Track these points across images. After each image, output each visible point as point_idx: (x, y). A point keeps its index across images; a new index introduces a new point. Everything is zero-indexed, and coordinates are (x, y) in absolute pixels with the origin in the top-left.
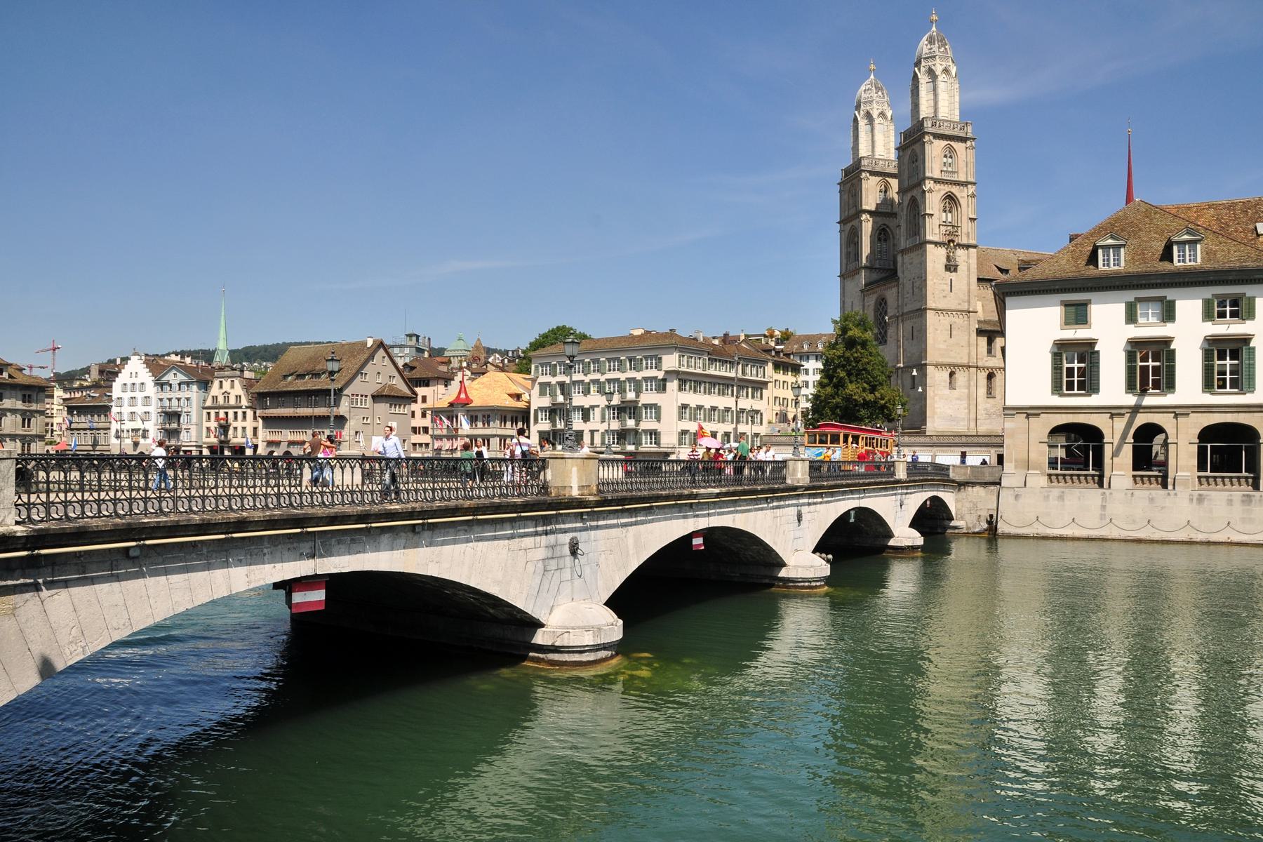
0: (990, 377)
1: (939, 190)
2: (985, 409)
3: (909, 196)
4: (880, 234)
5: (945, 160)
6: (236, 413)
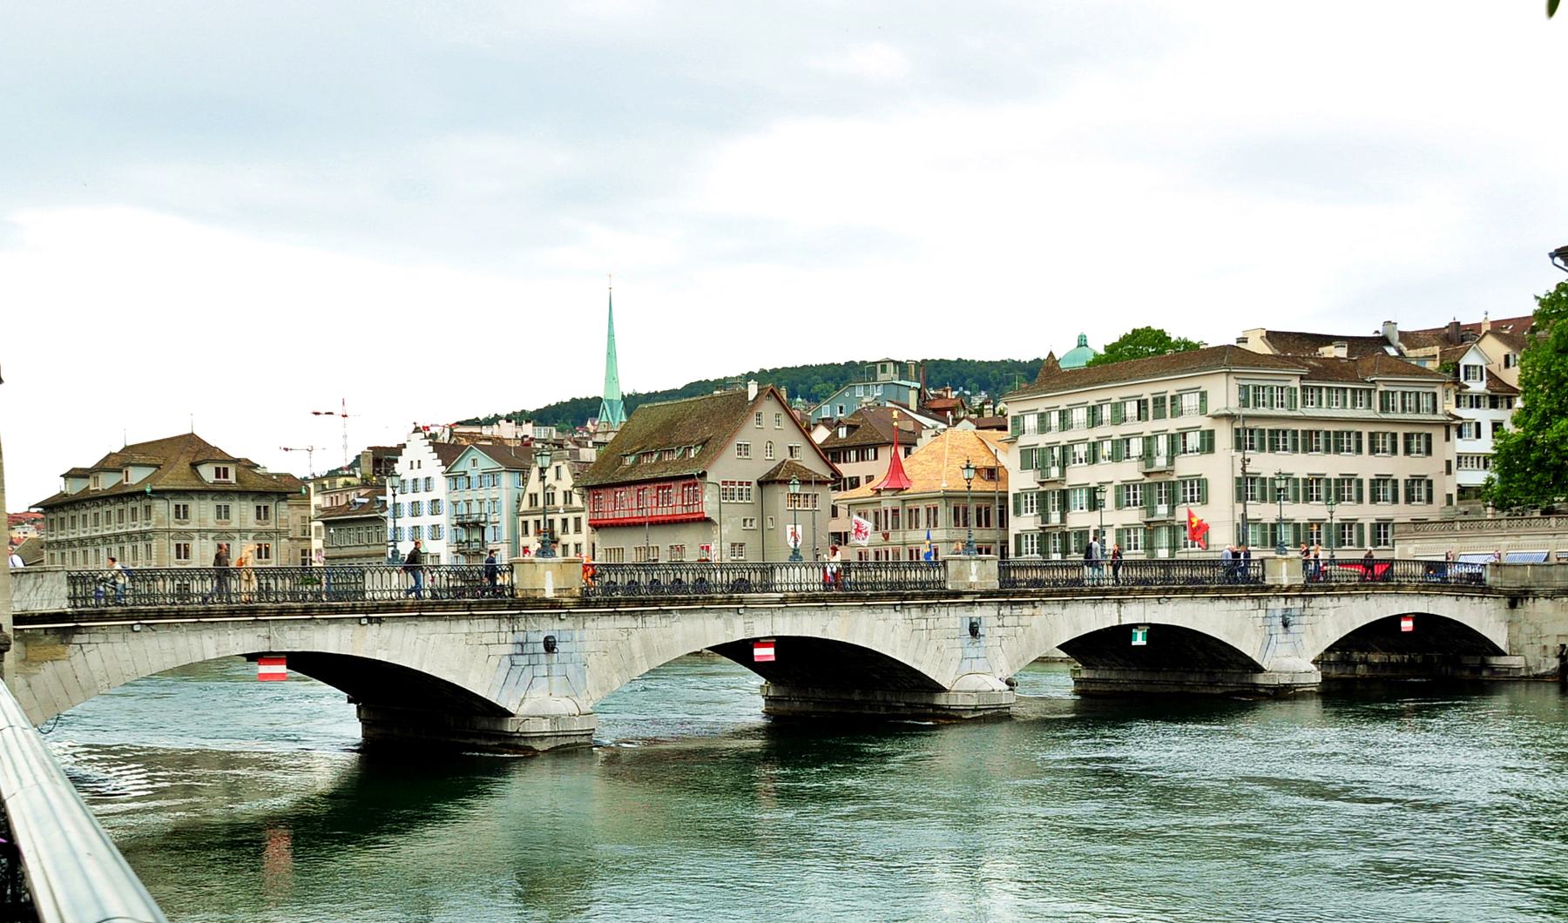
6: (565, 521)
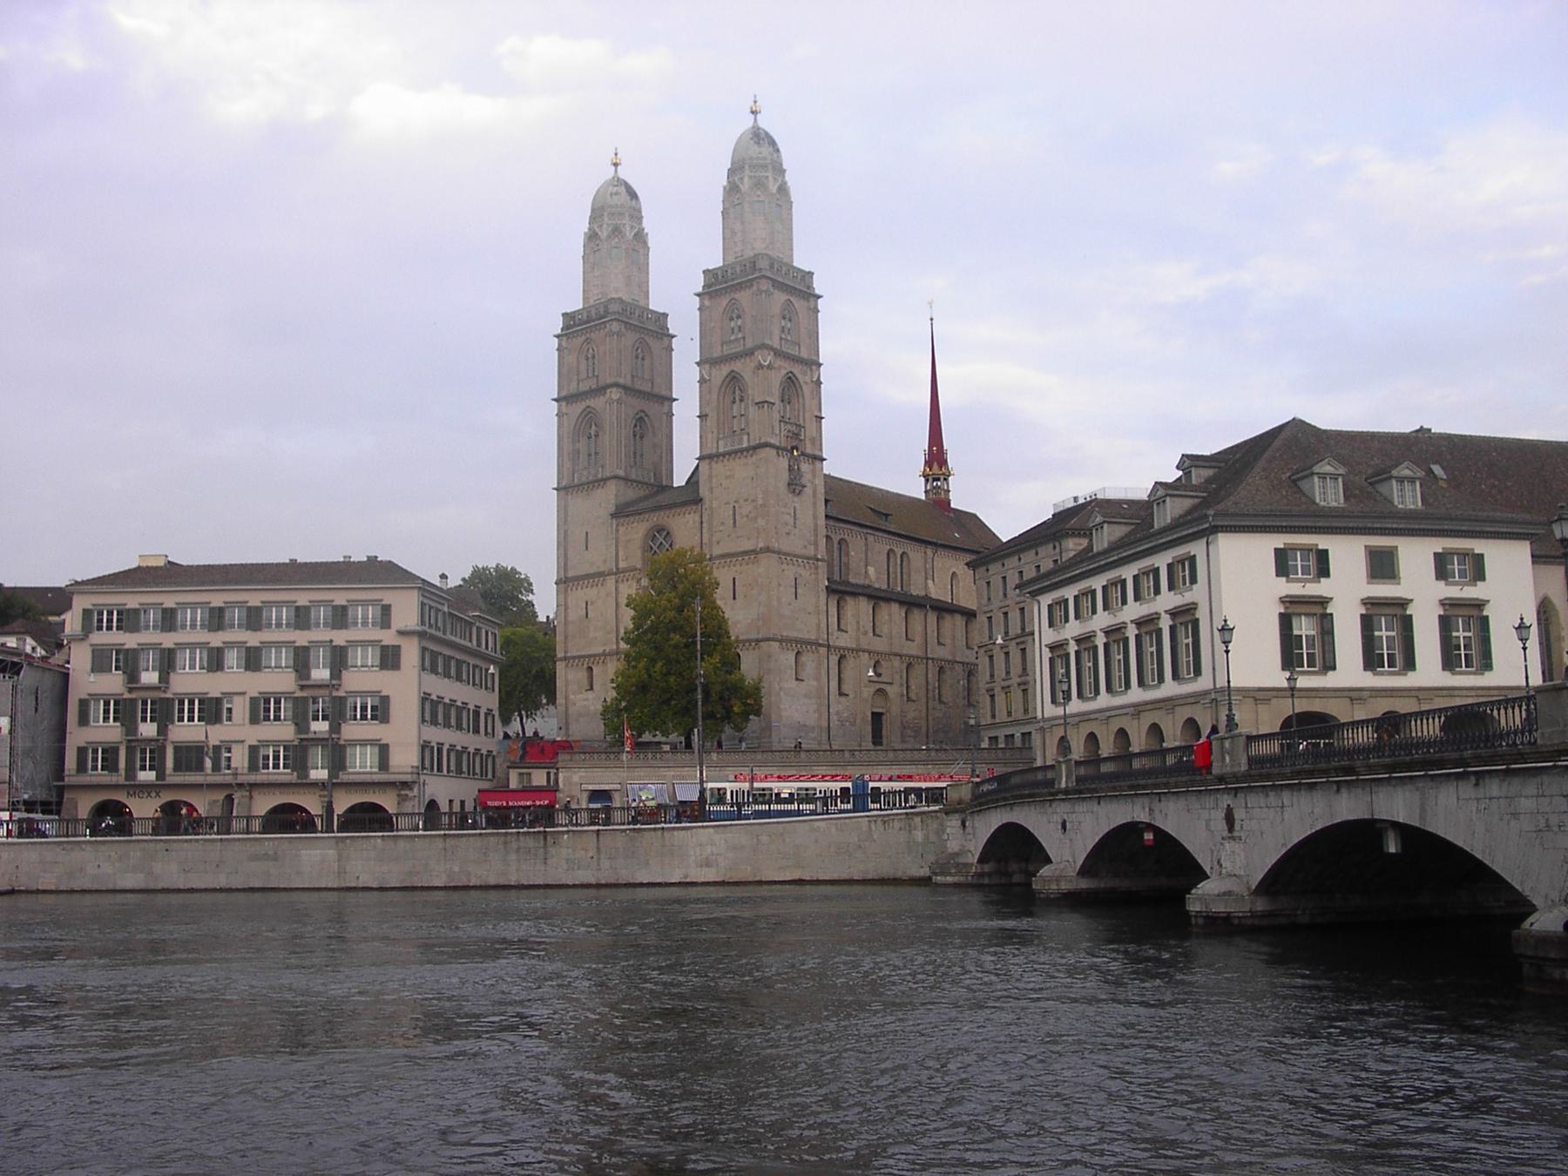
0: (842, 658)
1: (780, 368)
2: (838, 713)
3: (725, 370)
4: (635, 426)
5: (783, 323)
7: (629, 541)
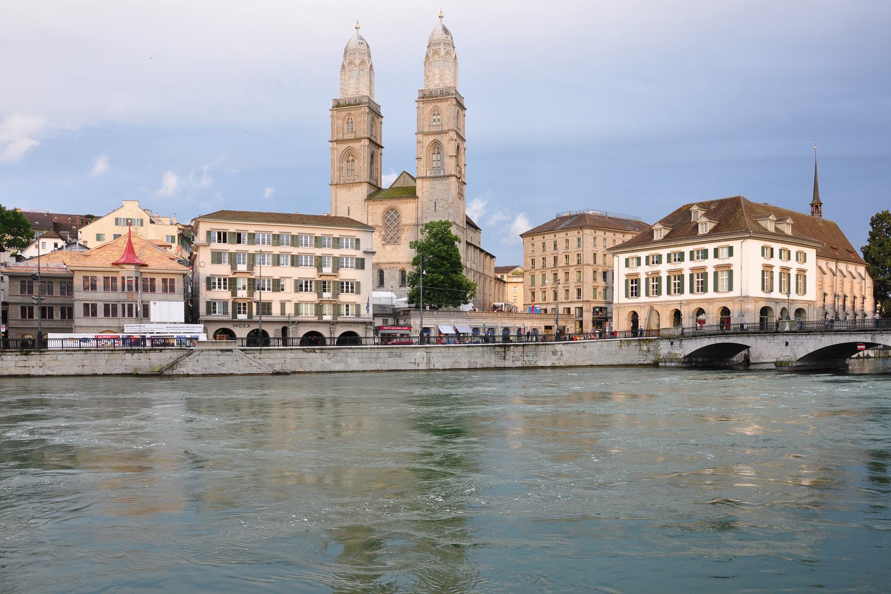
7: (373, 213)
